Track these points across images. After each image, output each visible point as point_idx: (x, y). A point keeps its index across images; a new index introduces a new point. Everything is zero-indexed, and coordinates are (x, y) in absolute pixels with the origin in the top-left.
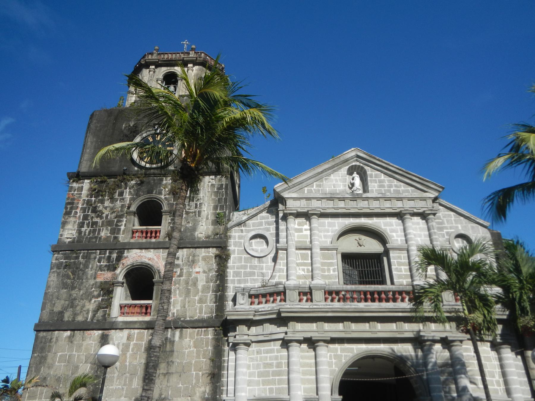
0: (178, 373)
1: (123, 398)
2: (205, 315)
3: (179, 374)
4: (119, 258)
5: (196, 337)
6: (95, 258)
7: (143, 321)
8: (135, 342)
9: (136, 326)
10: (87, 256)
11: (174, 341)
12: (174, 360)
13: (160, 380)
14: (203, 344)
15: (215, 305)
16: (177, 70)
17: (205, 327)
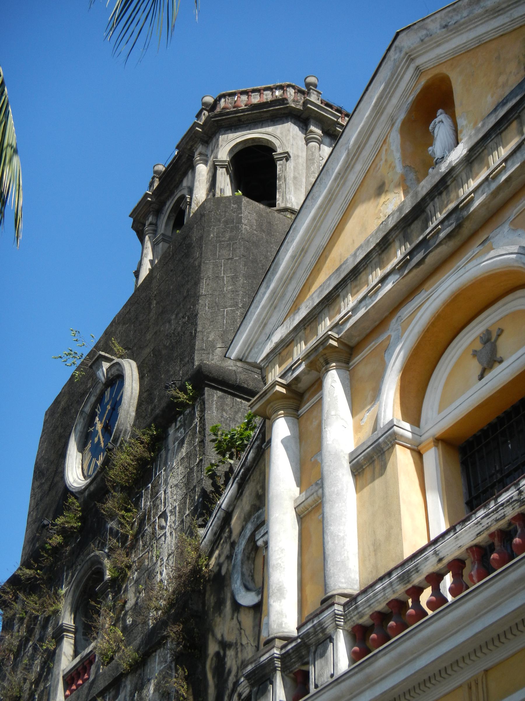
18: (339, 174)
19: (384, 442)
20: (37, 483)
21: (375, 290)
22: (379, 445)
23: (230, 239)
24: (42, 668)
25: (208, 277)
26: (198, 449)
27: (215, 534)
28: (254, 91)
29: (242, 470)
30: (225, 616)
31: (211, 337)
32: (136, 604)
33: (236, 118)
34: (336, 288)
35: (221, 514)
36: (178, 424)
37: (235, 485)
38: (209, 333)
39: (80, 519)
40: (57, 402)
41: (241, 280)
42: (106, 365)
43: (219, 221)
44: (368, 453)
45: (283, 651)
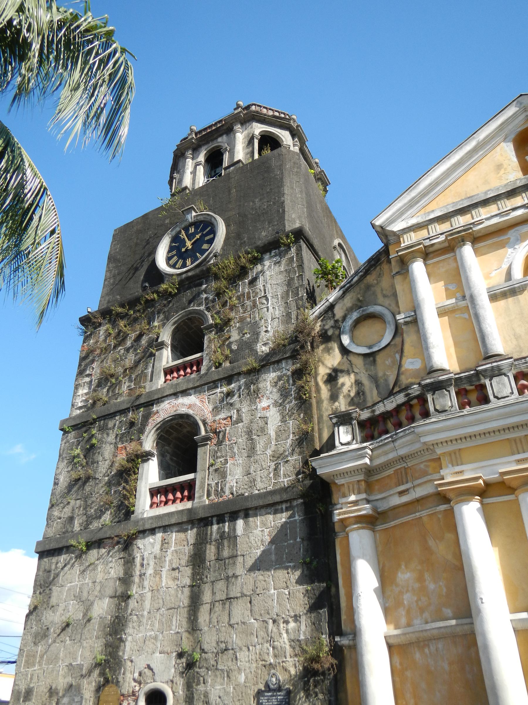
0: (246, 596)
1: (157, 654)
2: (286, 480)
3: (249, 598)
4: (146, 418)
5: (273, 523)
6: (115, 425)
7: (182, 511)
8: (173, 549)
9: (173, 521)
10: (103, 427)
11: (235, 537)
12: (238, 573)
13: (216, 614)
14: (286, 535)
15: (300, 457)
16: (222, 141)
17: (286, 501)
18: (469, 152)
19: (519, 287)
20: (111, 265)
21: (507, 213)
22: (514, 288)
23: (297, 172)
24: (137, 364)
25: (288, 186)
26: (296, 269)
27: (321, 314)
28: (270, 109)
29: (348, 285)
30: (334, 356)
31: (293, 216)
32: (241, 339)
33: (263, 118)
34: (469, 206)
35: (327, 304)
36: (273, 254)
37: (341, 292)
38: (292, 214)
39: (177, 288)
40: (128, 226)
41: (304, 195)
42: (194, 214)
43: (291, 161)
44: (504, 291)
45: (457, 376)
